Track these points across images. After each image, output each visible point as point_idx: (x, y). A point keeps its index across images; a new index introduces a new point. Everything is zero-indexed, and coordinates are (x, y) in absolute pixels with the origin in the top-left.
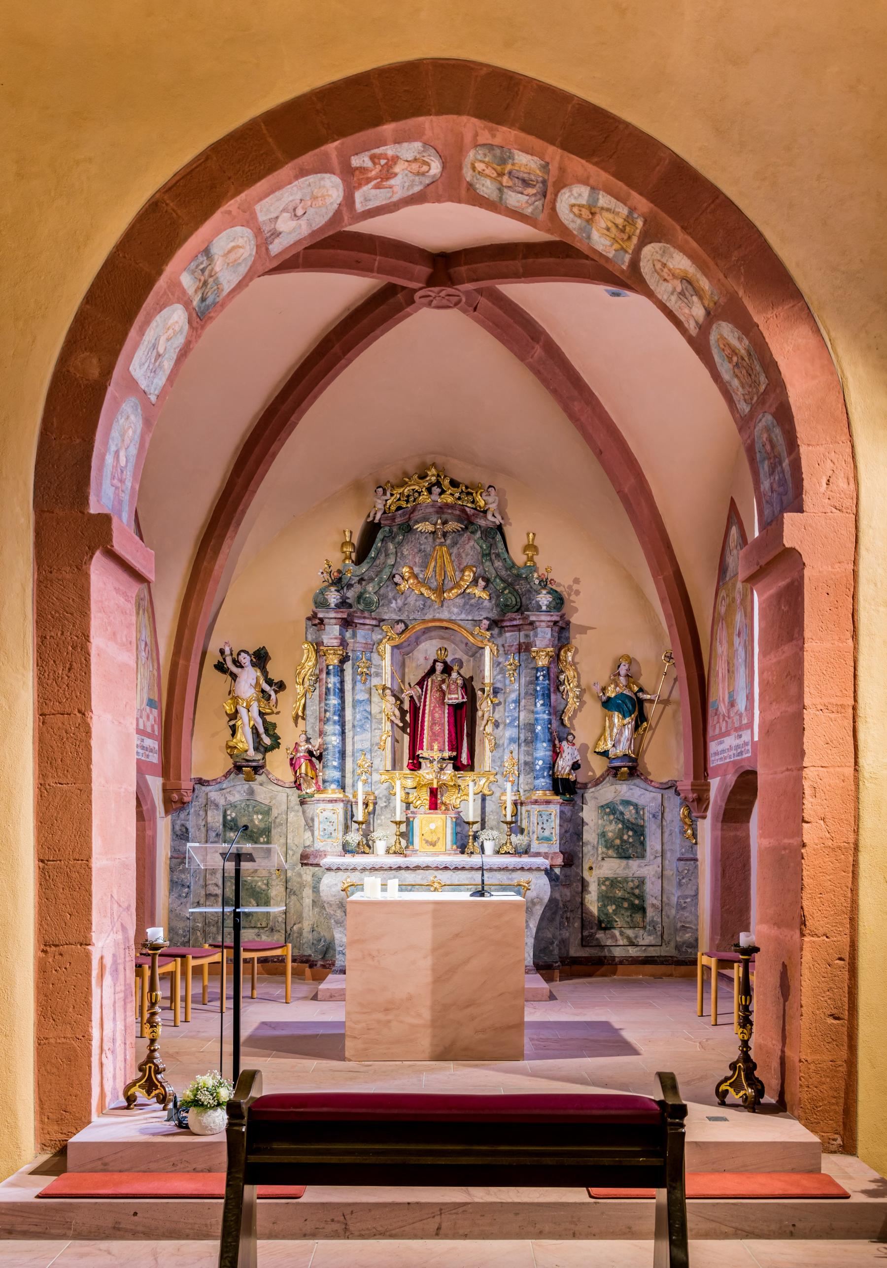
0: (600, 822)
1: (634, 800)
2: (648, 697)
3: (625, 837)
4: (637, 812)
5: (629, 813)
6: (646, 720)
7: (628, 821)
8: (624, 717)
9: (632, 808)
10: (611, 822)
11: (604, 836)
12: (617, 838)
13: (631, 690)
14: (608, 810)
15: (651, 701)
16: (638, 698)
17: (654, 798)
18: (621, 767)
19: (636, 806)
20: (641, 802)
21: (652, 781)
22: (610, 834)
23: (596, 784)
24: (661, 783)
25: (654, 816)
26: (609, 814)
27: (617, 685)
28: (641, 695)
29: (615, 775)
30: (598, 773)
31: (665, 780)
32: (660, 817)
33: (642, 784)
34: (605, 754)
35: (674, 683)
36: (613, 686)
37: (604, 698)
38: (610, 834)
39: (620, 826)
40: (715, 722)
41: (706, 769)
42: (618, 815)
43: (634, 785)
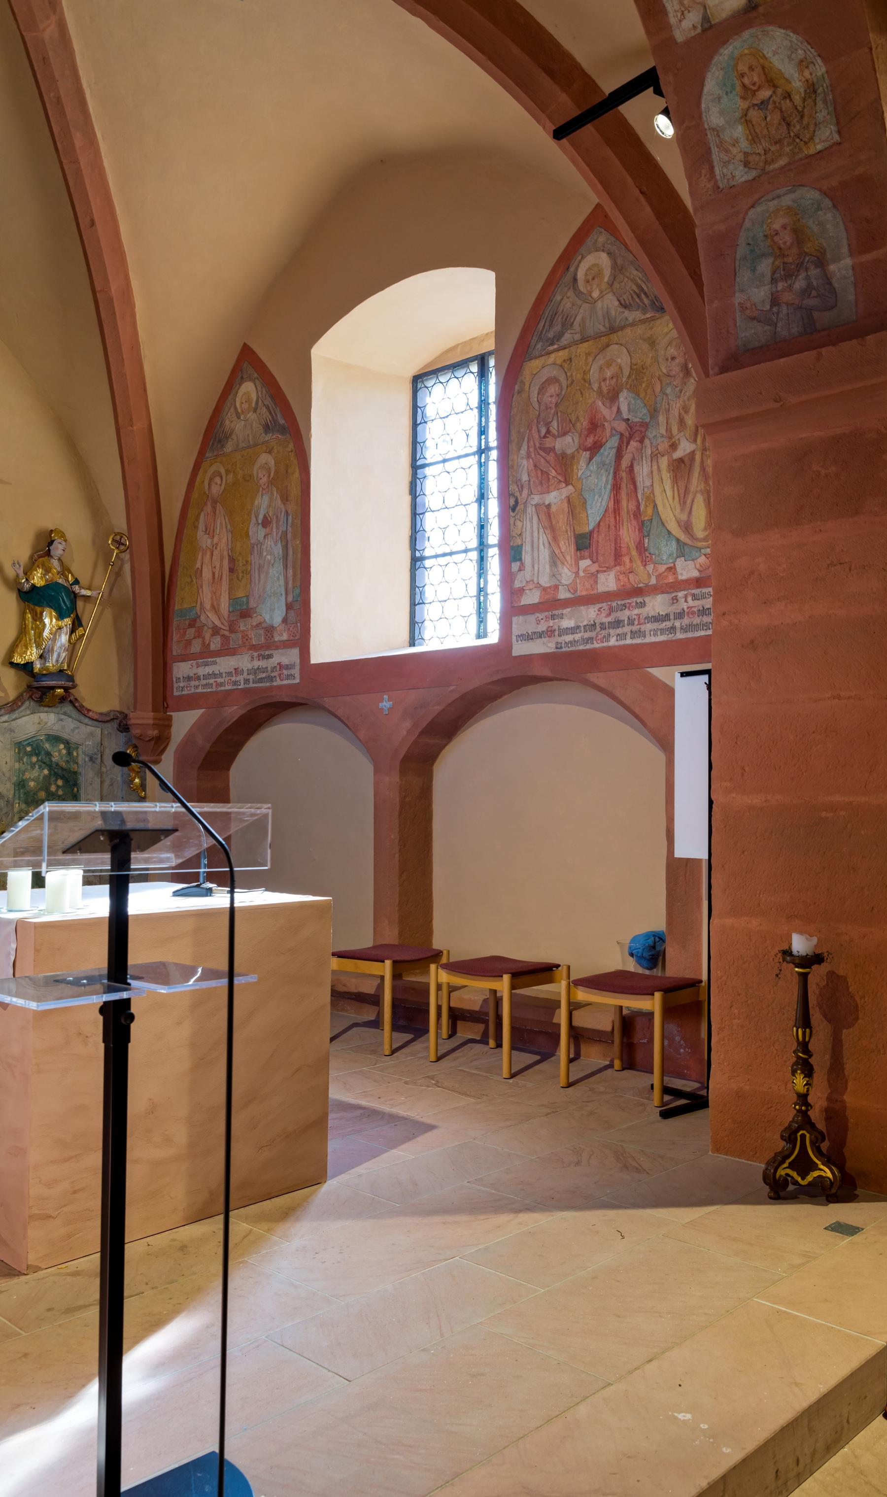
0: (17, 765)
1: (65, 736)
2: (88, 593)
3: (53, 788)
4: (69, 753)
5: (58, 753)
6: (81, 625)
7: (57, 765)
8: (60, 617)
9: (62, 746)
10: (33, 766)
11: (24, 786)
12: (41, 789)
13: (67, 580)
14: (29, 749)
15: (87, 598)
16: (74, 592)
17: (92, 734)
18: (53, 688)
19: (67, 743)
20: (75, 738)
21: (89, 710)
22: (32, 784)
23: (12, 711)
24: (101, 714)
25: (91, 759)
26: (30, 755)
27: (47, 571)
28: (76, 588)
29: (40, 701)
30: (12, 695)
31: (104, 710)
32: (99, 760)
33: (74, 713)
34: (27, 667)
35: (116, 579)
36: (40, 571)
37: (27, 587)
38: (32, 784)
39: (46, 772)
40: (187, 637)
41: (165, 698)
42: (42, 756)
43: (65, 714)
